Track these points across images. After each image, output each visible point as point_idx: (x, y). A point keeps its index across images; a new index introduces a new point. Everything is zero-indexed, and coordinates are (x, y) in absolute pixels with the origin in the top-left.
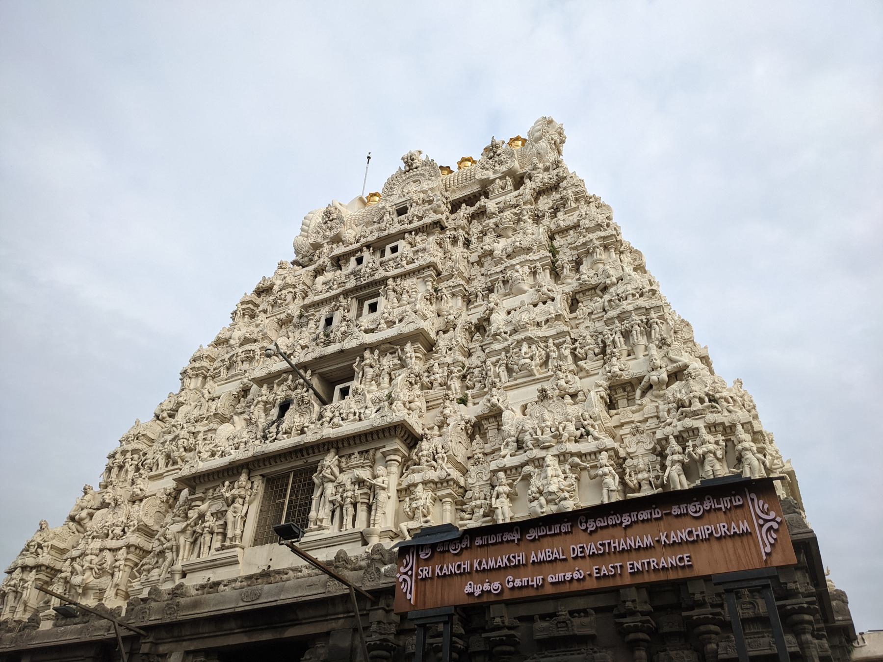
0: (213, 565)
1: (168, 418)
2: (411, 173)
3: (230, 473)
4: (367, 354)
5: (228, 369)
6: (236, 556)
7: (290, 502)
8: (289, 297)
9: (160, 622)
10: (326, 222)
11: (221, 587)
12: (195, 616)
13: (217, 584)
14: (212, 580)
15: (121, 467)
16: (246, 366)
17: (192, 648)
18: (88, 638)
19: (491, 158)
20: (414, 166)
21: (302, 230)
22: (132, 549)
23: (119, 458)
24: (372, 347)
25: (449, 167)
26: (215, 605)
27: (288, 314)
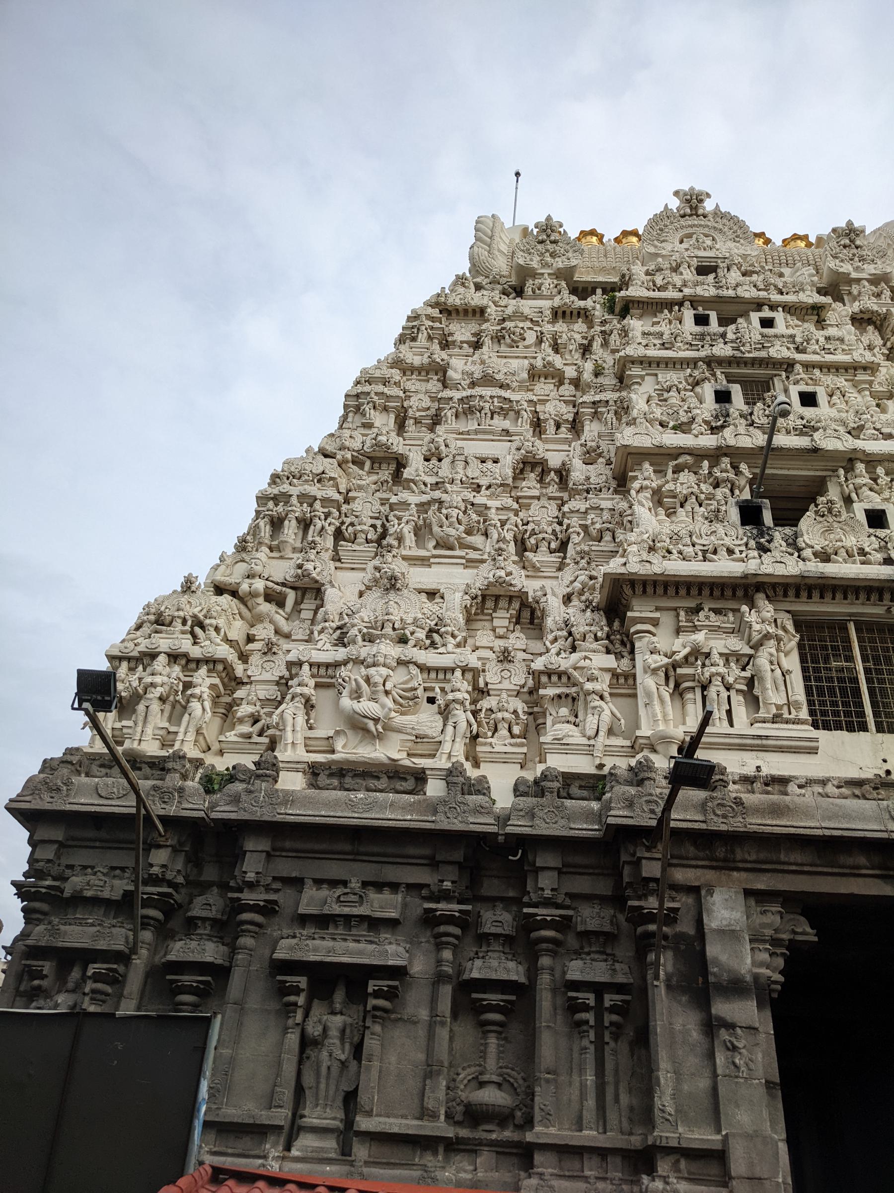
0: (760, 745)
1: (351, 465)
2: (695, 221)
3: (717, 593)
4: (860, 467)
5: (457, 417)
6: (816, 740)
7: (867, 671)
8: (531, 337)
9: (703, 826)
10: (542, 242)
11: (792, 788)
12: (792, 831)
13: (781, 782)
14: (765, 771)
15: (305, 524)
16: (500, 423)
17: (760, 886)
18: (457, 825)
19: (845, 247)
20: (700, 212)
21: (477, 239)
22: (469, 676)
23: (298, 509)
24: (872, 461)
25: (763, 234)
26: (824, 819)
27: (549, 363)
